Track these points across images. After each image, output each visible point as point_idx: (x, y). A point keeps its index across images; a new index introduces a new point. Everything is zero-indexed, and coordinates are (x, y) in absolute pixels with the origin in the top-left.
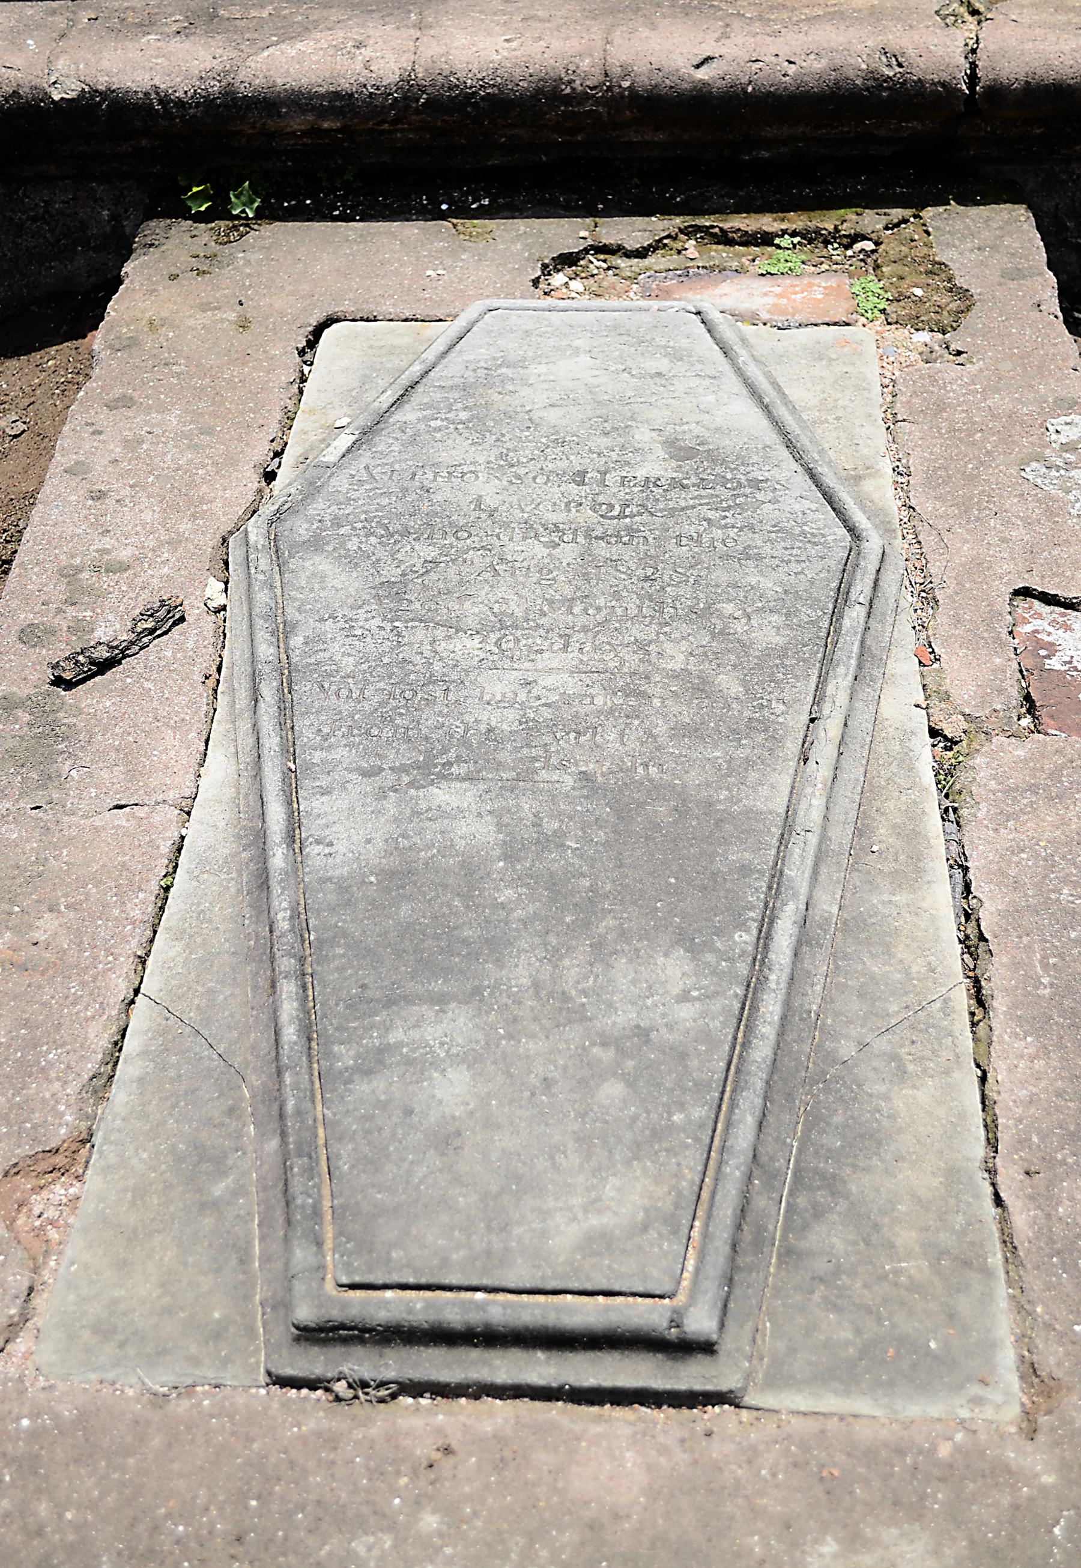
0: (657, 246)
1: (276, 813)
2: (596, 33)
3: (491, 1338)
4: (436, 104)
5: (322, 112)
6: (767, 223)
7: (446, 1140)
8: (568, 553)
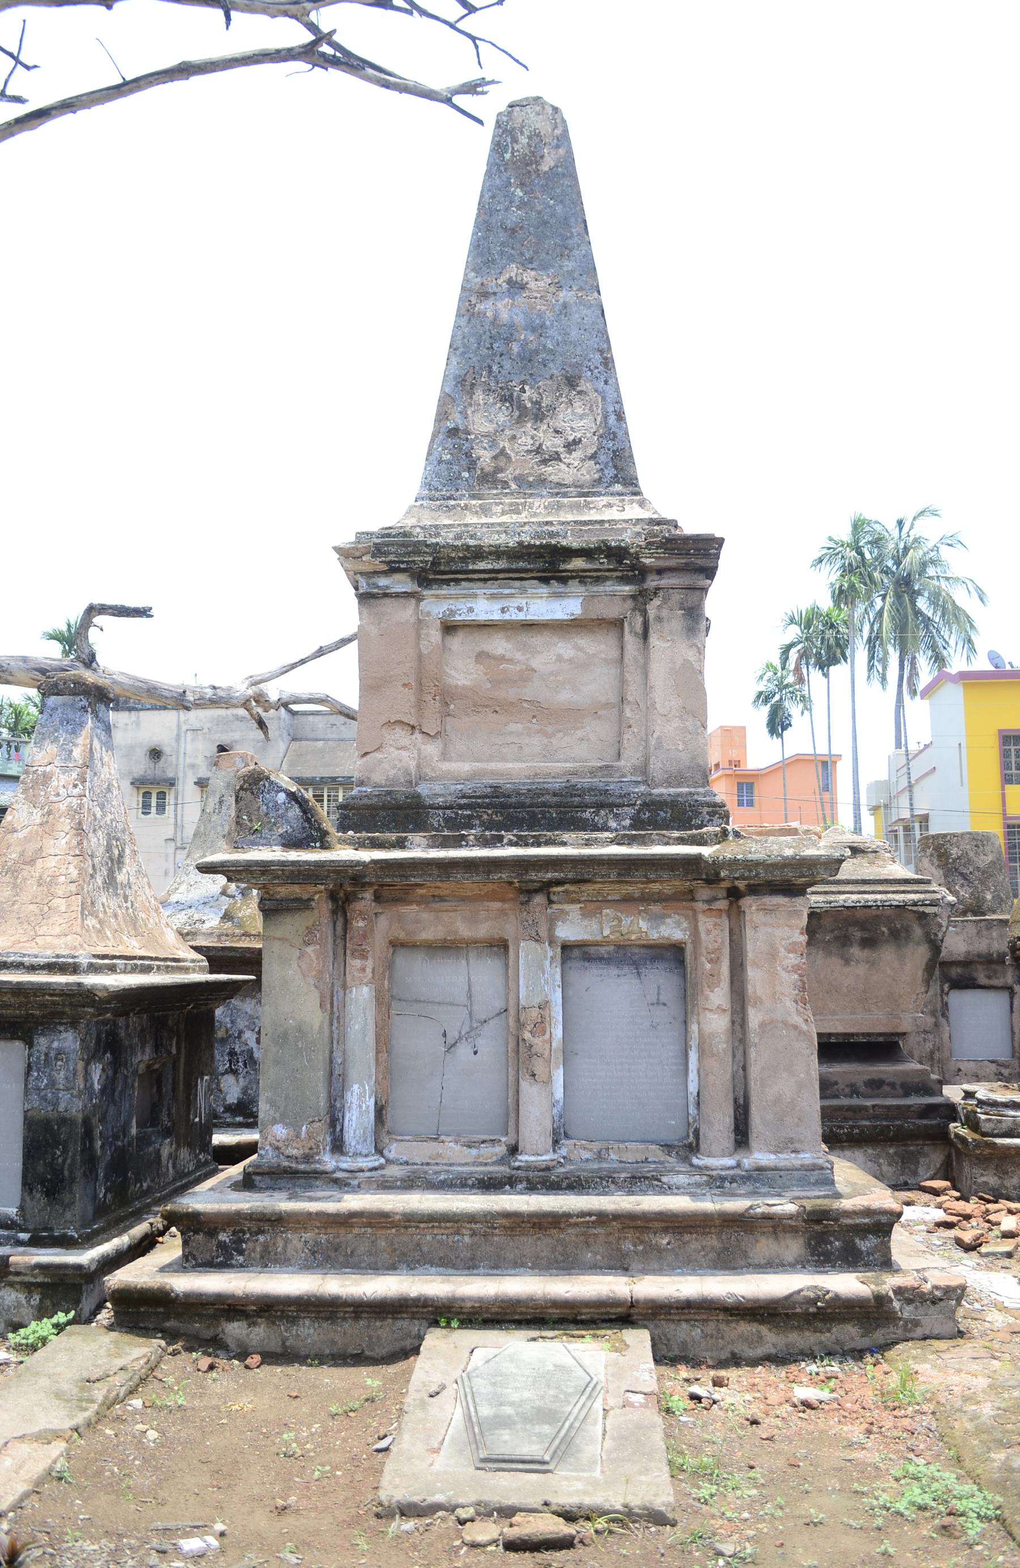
1: (472, 1409)
2: (542, 1286)
3: (512, 1461)
4: (502, 1301)
5: (475, 1302)
6: (583, 1332)
7: (505, 1442)
8: (531, 1379)
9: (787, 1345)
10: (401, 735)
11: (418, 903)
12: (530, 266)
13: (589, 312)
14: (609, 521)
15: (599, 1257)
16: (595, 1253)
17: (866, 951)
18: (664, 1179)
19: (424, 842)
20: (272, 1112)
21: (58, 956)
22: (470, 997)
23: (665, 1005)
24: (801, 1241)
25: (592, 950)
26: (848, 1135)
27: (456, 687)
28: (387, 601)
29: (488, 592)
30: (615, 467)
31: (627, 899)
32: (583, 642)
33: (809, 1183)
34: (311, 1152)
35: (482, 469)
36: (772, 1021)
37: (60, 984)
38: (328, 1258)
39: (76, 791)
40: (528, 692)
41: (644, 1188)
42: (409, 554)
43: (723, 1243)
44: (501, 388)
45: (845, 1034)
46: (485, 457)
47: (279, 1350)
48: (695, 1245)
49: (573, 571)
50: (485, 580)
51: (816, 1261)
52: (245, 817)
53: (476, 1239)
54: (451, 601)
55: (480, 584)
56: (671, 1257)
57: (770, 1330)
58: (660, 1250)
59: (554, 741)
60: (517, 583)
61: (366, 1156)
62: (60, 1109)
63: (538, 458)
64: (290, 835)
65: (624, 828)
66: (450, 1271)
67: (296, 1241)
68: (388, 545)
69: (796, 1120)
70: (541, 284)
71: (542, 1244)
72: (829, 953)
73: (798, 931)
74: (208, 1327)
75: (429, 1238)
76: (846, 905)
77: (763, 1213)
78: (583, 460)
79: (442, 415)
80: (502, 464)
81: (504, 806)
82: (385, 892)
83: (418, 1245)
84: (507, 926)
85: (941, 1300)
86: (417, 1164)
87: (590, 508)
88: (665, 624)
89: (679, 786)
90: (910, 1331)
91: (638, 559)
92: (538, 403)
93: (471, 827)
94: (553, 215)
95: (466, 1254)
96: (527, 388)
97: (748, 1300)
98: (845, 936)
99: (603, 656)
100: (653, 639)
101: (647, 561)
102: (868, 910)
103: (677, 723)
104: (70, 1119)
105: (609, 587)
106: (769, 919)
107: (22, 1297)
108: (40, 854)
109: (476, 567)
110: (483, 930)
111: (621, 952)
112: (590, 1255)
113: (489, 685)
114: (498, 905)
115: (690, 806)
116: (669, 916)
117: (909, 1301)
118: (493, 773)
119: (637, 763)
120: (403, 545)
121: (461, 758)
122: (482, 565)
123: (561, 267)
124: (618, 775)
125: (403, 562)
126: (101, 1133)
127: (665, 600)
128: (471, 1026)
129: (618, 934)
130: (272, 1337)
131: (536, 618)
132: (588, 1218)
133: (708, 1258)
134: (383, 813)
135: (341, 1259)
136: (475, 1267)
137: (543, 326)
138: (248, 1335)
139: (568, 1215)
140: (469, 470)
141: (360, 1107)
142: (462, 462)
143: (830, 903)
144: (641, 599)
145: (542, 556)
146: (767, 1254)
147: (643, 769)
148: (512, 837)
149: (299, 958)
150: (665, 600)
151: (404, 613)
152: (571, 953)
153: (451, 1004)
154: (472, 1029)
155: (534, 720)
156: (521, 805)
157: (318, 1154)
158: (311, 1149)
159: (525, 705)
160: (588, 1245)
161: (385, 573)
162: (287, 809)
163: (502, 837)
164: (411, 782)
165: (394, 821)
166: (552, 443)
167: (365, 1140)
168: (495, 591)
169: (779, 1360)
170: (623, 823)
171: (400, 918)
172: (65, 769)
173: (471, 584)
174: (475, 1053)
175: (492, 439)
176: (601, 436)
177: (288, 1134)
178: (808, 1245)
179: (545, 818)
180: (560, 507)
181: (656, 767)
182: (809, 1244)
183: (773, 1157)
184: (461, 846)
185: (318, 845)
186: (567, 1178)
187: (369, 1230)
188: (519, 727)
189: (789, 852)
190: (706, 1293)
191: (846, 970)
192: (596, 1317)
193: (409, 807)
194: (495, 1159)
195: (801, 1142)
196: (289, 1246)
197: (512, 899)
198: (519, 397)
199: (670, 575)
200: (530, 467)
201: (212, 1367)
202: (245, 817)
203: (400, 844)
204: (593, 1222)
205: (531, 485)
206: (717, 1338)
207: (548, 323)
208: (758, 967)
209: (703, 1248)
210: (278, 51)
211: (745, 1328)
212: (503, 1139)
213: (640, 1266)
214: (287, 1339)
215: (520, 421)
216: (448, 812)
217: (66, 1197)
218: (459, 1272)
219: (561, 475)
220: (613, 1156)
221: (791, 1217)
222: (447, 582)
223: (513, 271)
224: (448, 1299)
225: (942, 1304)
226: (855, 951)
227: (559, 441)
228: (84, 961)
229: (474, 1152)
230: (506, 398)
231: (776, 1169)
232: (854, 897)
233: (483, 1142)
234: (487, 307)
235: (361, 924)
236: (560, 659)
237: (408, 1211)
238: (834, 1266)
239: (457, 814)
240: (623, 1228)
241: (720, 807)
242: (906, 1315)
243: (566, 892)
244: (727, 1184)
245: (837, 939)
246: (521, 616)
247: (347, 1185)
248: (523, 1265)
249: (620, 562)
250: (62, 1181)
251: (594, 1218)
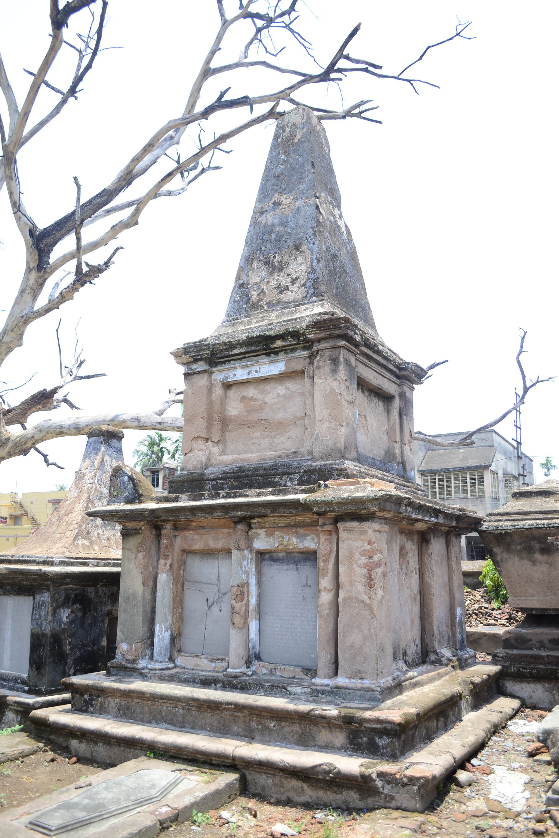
0: (192, 771)
4: (174, 746)
9: (317, 798)
10: (200, 444)
11: (193, 530)
12: (284, 192)
13: (308, 209)
14: (299, 318)
15: (240, 730)
16: (239, 727)
17: (545, 556)
18: (289, 689)
19: (186, 498)
20: (122, 636)
21: (48, 558)
22: (219, 580)
23: (310, 586)
24: (345, 734)
25: (275, 555)
26: (529, 673)
27: (231, 416)
28: (196, 376)
29: (241, 365)
30: (314, 288)
31: (288, 526)
32: (289, 385)
33: (366, 699)
36: (350, 598)
37: (33, 570)
38: (124, 713)
39: (92, 481)
40: (263, 416)
41: (277, 692)
42: (199, 351)
43: (302, 730)
44: (265, 258)
45: (542, 609)
46: (254, 295)
47: (90, 757)
48: (287, 729)
49: (279, 348)
50: (241, 359)
51: (353, 749)
53: (185, 711)
54: (226, 372)
55: (239, 361)
56: (275, 735)
57: (308, 787)
58: (270, 730)
59: (275, 440)
60: (256, 358)
61: (161, 662)
63: (279, 290)
64: (128, 497)
65: (295, 485)
66: (173, 728)
67: (113, 703)
68: (189, 348)
69: (363, 659)
70: (288, 200)
72: (521, 558)
73: (367, 543)
74: (65, 741)
76: (525, 527)
77: (319, 714)
78: (299, 287)
79: (238, 277)
80: (262, 297)
81: (239, 477)
82: (179, 524)
83: (161, 711)
85: (407, 785)
87: (297, 312)
88: (321, 370)
89: (327, 460)
90: (388, 802)
91: (305, 336)
92: (281, 262)
93: (223, 489)
94: (297, 163)
95: (180, 719)
96: (277, 255)
97: (291, 766)
98: (529, 547)
99: (299, 391)
102: (540, 530)
103: (327, 424)
106: (349, 536)
107: (15, 716)
108: (71, 511)
109: (233, 353)
110: (220, 544)
111: (288, 555)
112: (236, 728)
113: (246, 413)
114: (226, 530)
115: (328, 471)
116: (309, 535)
117: (389, 783)
118: (242, 460)
121: (232, 453)
122: (235, 351)
123: (298, 189)
124: (300, 456)
125: (198, 355)
126: (69, 642)
127: (322, 356)
128: (219, 596)
131: (263, 375)
132: (230, 706)
133: (294, 738)
134: (186, 484)
135: (130, 714)
136: (184, 727)
137: (287, 222)
140: (247, 303)
141: (159, 636)
142: (244, 300)
143: (515, 526)
145: (261, 342)
146: (325, 740)
147: (311, 452)
148: (224, 494)
149: (135, 558)
151: (202, 381)
152: (262, 556)
153: (210, 584)
154: (219, 598)
155: (266, 430)
156: (247, 476)
159: (262, 422)
160: (235, 722)
163: (220, 493)
164: (202, 467)
165: (191, 488)
166: (285, 281)
167: (161, 654)
168: (244, 364)
169: (308, 806)
170: (294, 483)
172: (91, 471)
173: (235, 362)
174: (220, 611)
175: (258, 285)
176: (309, 273)
178: (348, 737)
179: (256, 482)
180: (283, 314)
182: (349, 737)
183: (348, 681)
184: (202, 499)
186: (240, 683)
187: (140, 701)
188: (259, 434)
189: (346, 495)
190: (269, 758)
191: (535, 568)
192: (221, 763)
193: (197, 480)
195: (365, 673)
198: (272, 261)
199: (324, 342)
200: (271, 295)
201: (53, 760)
204: (232, 709)
205: (273, 306)
206: (280, 787)
207: (289, 219)
209: (292, 731)
210: (259, 118)
211: (295, 783)
213: (260, 738)
215: (272, 273)
217: (43, 671)
218: (177, 729)
219: (288, 297)
220: (278, 673)
221: (335, 718)
222: (224, 362)
223: (276, 197)
224: (151, 741)
225: (408, 787)
226: (538, 556)
227: (289, 280)
228: (57, 560)
229: (213, 664)
231: (346, 688)
232: (530, 522)
233: (218, 660)
234: (262, 219)
235: (165, 541)
236: (278, 395)
237: (152, 692)
238: (362, 753)
239: (217, 482)
240: (251, 714)
241: (344, 471)
242: (386, 791)
243: (258, 522)
244: (320, 695)
245: (524, 548)
246: (257, 375)
247: (146, 676)
248: (205, 729)
249: (299, 339)
250: (42, 663)
251: (233, 706)
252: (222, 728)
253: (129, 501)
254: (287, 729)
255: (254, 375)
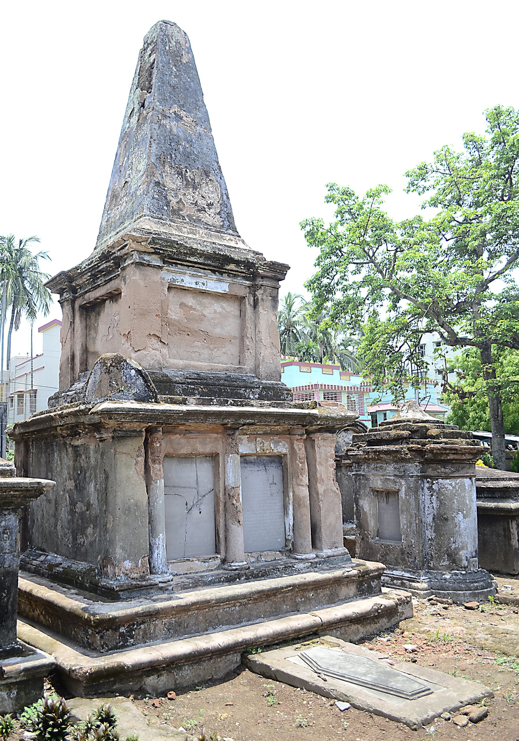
15: (288, 607)
20: (123, 554)
25: (248, 458)
28: (149, 268)
31: (265, 434)
32: (224, 305)
34: (144, 574)
35: (173, 207)
42: (166, 246)
52: (114, 382)
54: (174, 274)
55: (186, 268)
56: (313, 602)
60: (202, 271)
62: (6, 566)
67: (160, 624)
71: (265, 606)
75: (221, 611)
84: (218, 446)
86: (181, 575)
100: (260, 309)
101: (261, 271)
103: (269, 350)
104: (12, 572)
105: (239, 280)
106: (325, 443)
110: (208, 449)
111: (259, 459)
113: (186, 321)
118: (194, 367)
119: (252, 367)
120: (167, 241)
124: (244, 372)
125: (161, 250)
129: (262, 450)
130: (170, 680)
131: (210, 290)
132: (289, 588)
135: (182, 630)
138: (158, 682)
139: (282, 588)
144: (253, 288)
150: (265, 291)
152: (245, 459)
153: (189, 488)
154: (199, 500)
155: (205, 341)
157: (147, 575)
158: (144, 572)
161: (149, 253)
162: (136, 379)
171: (171, 442)
173: (183, 267)
174: (200, 513)
177: (132, 565)
179: (225, 392)
181: (262, 370)
185: (153, 400)
194: (216, 567)
196: (157, 628)
197: (221, 433)
199: (266, 279)
202: (114, 382)
203: (184, 402)
204: (291, 590)
208: (321, 465)
211: (354, 627)
212: (219, 556)
214: (177, 679)
216: (184, 385)
220: (263, 559)
229: (207, 564)
230: (180, 174)
236: (215, 312)
237: (218, 598)
239: (188, 387)
252: (274, 610)
253: (140, 399)
254: (321, 595)
255: (200, 287)
